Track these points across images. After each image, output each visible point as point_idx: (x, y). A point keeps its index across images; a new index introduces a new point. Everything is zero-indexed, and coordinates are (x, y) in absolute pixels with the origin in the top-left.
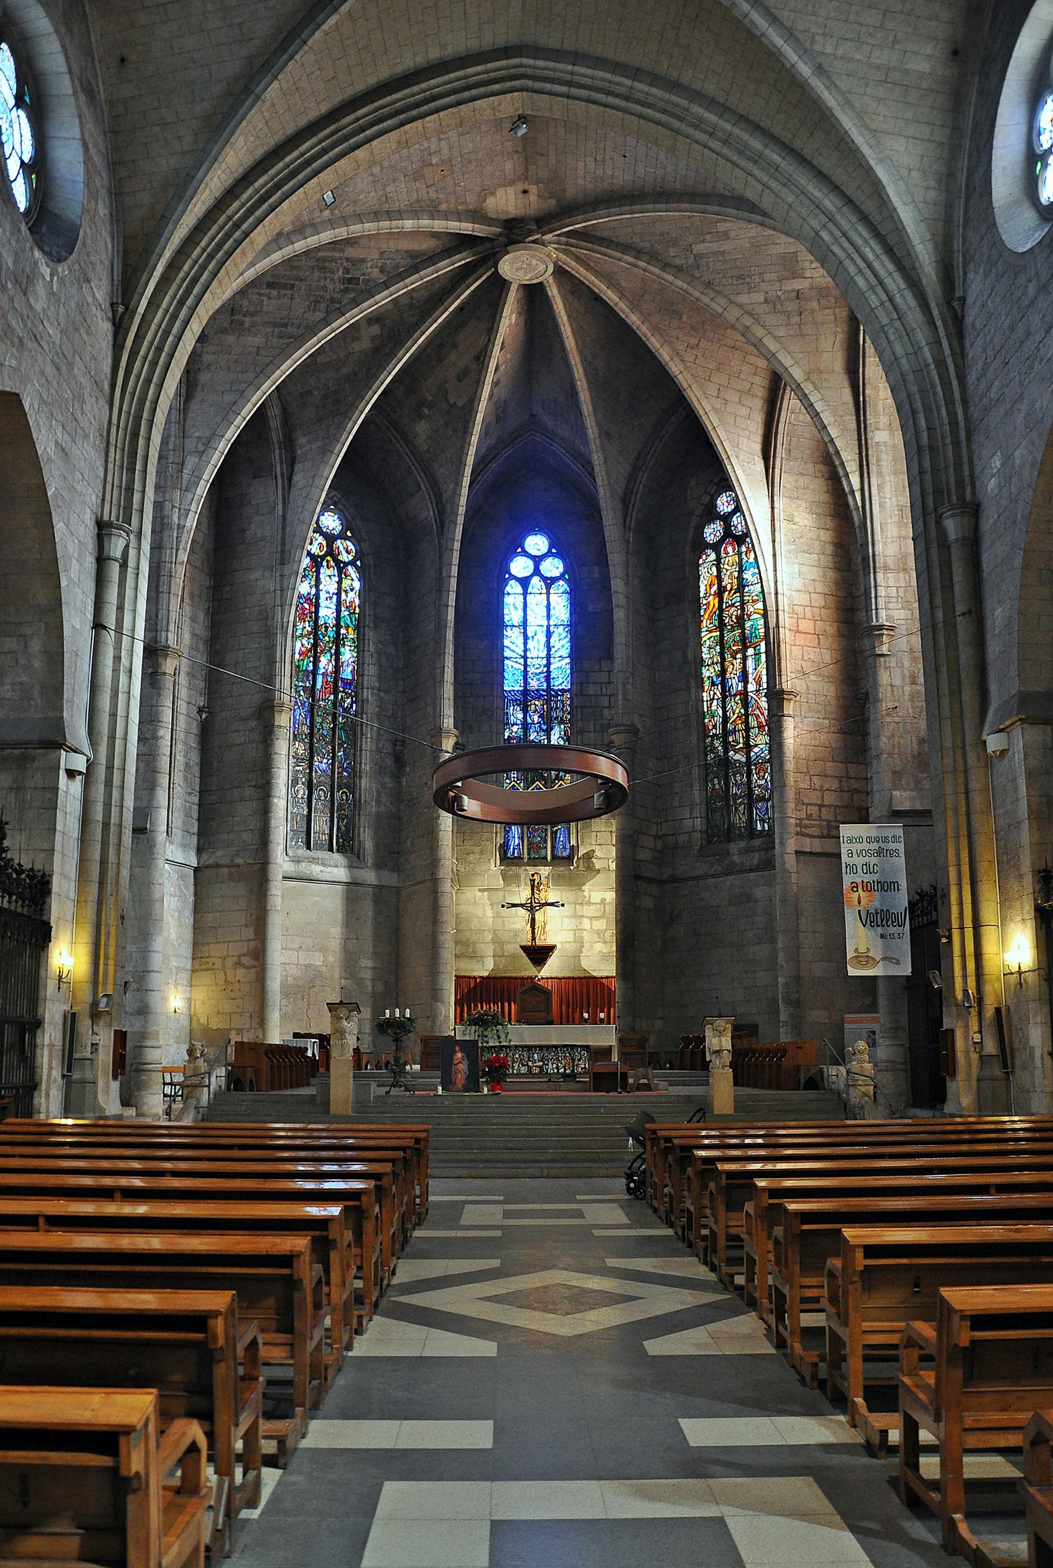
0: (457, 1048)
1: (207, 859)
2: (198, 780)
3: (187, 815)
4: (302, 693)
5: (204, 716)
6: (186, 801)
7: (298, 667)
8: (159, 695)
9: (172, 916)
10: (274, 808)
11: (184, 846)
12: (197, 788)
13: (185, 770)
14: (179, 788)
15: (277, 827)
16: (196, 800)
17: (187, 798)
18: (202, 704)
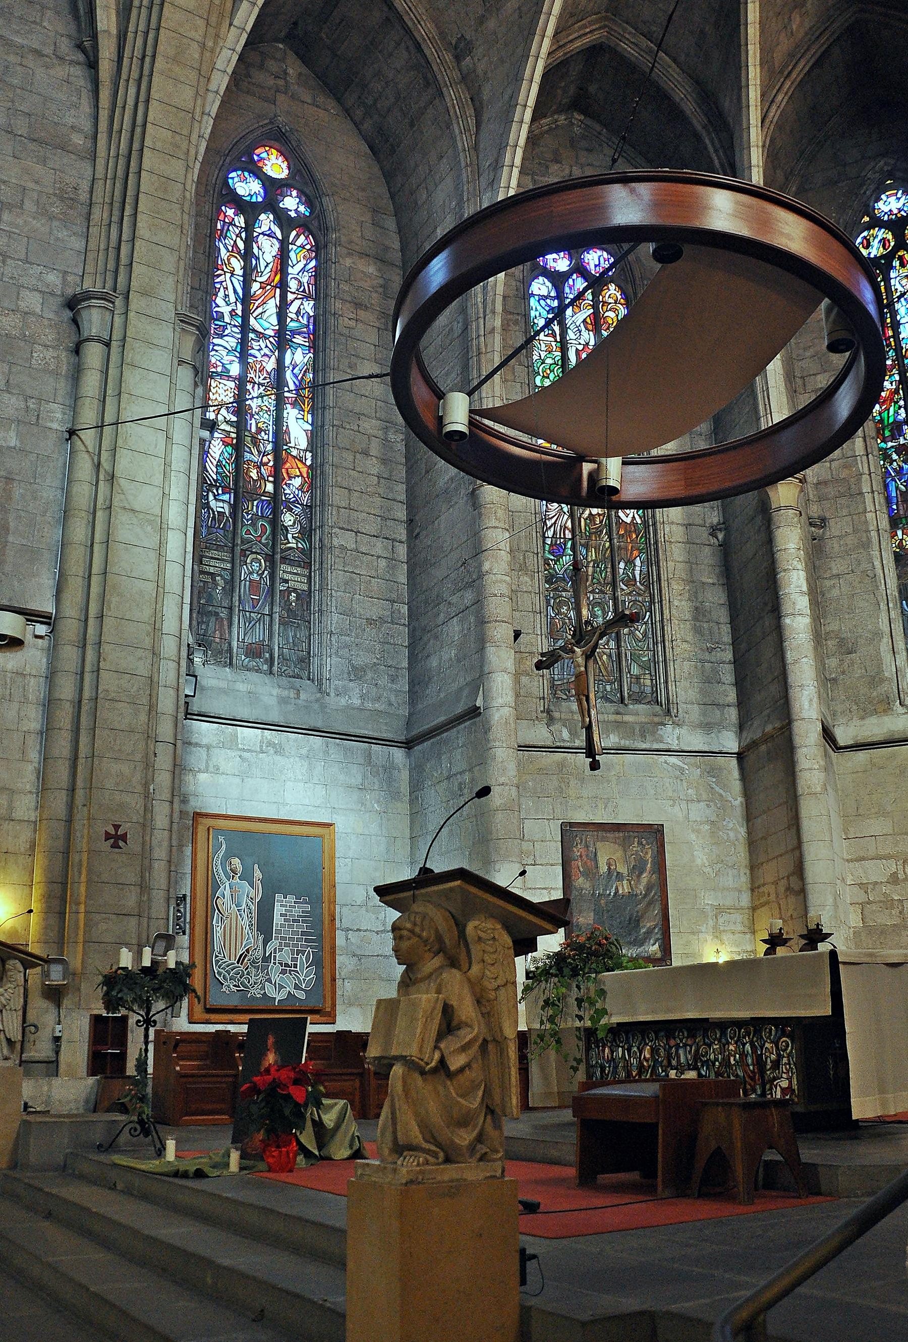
0: (271, 1040)
1: (749, 736)
2: (726, 629)
3: (709, 679)
4: (895, 457)
5: (721, 536)
6: (702, 661)
7: (881, 421)
8: (480, 515)
9: (698, 831)
10: (787, 633)
11: (707, 727)
12: (727, 639)
13: (696, 619)
14: (685, 646)
15: (796, 662)
16: (729, 656)
17: (707, 656)
18: (715, 520)
